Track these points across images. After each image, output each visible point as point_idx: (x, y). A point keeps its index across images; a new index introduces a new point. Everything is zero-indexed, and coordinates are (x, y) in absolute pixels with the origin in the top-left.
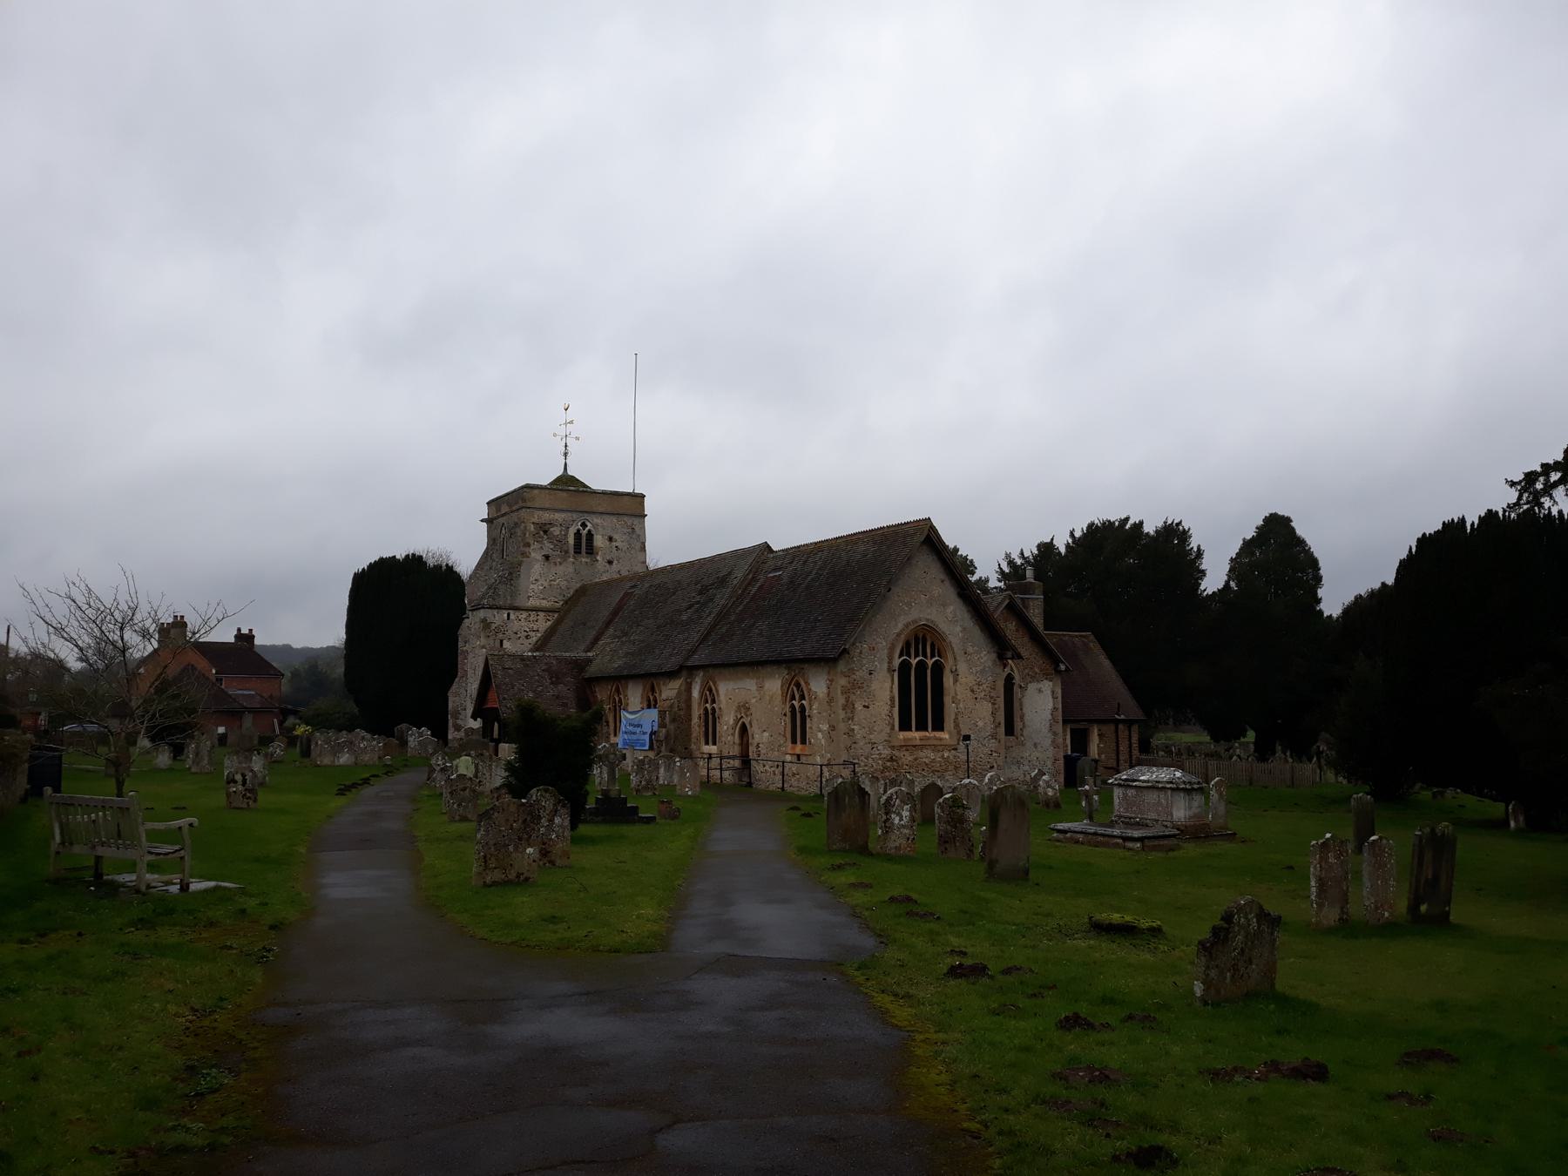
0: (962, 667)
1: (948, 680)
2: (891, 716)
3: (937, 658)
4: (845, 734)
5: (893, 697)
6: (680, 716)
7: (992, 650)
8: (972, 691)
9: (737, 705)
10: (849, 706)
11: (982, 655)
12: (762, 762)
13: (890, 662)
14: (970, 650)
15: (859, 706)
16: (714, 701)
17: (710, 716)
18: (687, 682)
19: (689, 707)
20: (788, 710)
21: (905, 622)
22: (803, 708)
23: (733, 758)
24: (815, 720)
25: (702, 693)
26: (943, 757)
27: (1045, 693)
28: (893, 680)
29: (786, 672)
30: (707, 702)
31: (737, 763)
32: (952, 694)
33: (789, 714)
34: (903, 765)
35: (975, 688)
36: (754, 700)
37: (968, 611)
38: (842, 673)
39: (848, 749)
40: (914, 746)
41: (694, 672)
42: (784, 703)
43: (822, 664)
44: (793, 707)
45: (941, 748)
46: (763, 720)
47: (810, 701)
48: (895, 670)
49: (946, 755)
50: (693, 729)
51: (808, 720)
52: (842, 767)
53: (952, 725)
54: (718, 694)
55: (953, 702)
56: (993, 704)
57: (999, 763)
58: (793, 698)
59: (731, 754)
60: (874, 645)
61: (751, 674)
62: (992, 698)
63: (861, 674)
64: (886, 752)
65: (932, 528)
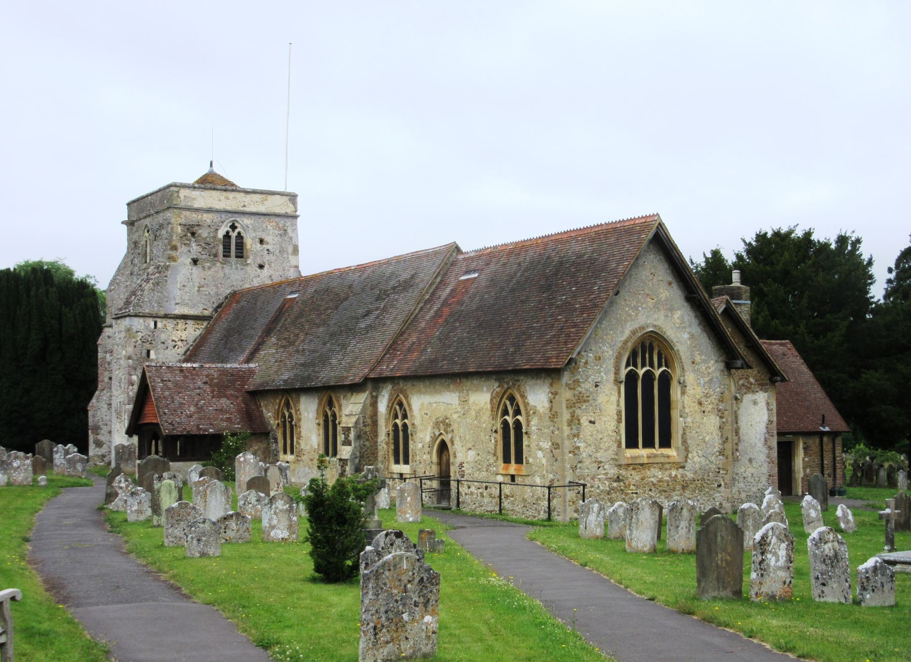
0: (690, 378)
1: (675, 393)
2: (618, 433)
3: (664, 368)
4: (570, 452)
5: (620, 412)
6: (365, 433)
7: (720, 359)
8: (700, 404)
9: (434, 420)
10: (574, 421)
11: (709, 365)
12: (466, 483)
13: (617, 372)
14: (698, 359)
15: (584, 421)
16: (405, 416)
17: (401, 434)
18: (372, 397)
19: (375, 423)
20: (499, 426)
21: (631, 329)
22: (518, 425)
23: (431, 479)
24: (534, 437)
25: (390, 408)
26: (670, 476)
27: (760, 405)
28: (619, 393)
29: (497, 384)
30: (396, 417)
31: (435, 484)
32: (680, 406)
33: (500, 431)
34: (629, 485)
35: (703, 400)
37: (696, 317)
38: (567, 385)
39: (574, 468)
40: (642, 465)
41: (381, 385)
42: (494, 418)
43: (543, 375)
44: (505, 424)
45: (667, 466)
46: (467, 438)
47: (528, 415)
48: (621, 382)
49: (674, 473)
50: (380, 448)
51: (525, 438)
52: (567, 488)
53: (680, 442)
54: (411, 409)
55: (681, 416)
56: (721, 417)
57: (726, 481)
58: (505, 412)
59: (428, 474)
60: (600, 354)
61: (451, 386)
62: (719, 411)
63: (587, 386)
64: (613, 471)
65: (661, 225)
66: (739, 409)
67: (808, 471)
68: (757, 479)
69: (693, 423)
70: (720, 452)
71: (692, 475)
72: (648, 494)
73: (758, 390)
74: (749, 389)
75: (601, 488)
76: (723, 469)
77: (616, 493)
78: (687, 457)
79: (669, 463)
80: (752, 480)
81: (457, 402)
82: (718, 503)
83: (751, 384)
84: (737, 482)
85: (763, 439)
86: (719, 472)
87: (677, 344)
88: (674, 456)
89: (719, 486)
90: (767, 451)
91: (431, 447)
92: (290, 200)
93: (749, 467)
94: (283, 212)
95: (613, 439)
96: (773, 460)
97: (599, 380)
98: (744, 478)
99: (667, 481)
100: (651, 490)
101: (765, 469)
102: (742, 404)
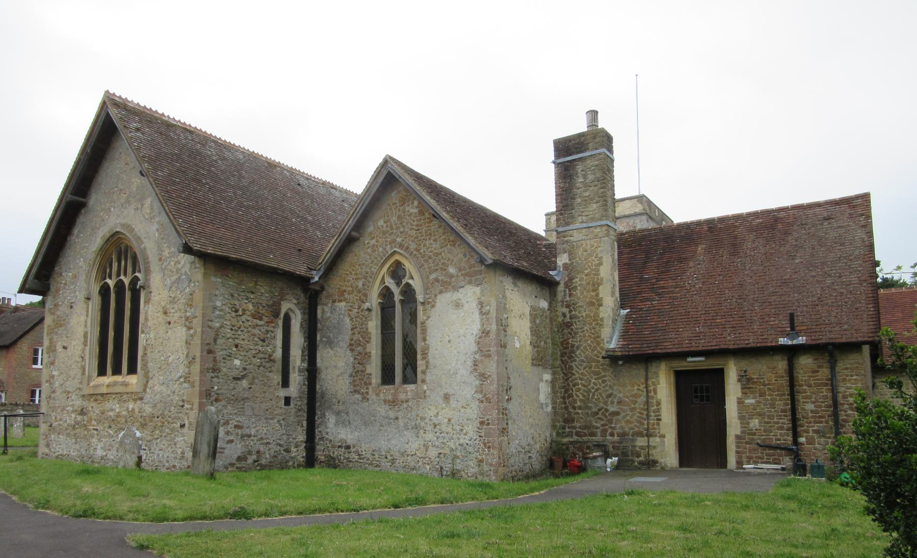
8: (165, 313)
15: (59, 349)
34: (91, 420)
40: (102, 395)
49: (131, 406)
56: (189, 328)
57: (190, 420)
63: (63, 310)
64: (78, 403)
66: (429, 317)
67: (755, 423)
68: (458, 428)
69: (155, 339)
70: (186, 378)
71: (150, 410)
72: (107, 432)
73: (463, 284)
74: (448, 285)
75: (68, 421)
76: (188, 402)
77: (80, 428)
78: (146, 386)
79: (128, 393)
80: (450, 430)
82: (179, 451)
83: (451, 276)
84: (422, 431)
85: (470, 363)
86: (183, 406)
87: (144, 240)
88: (132, 385)
89: (182, 426)
90: (477, 382)
92: (638, 201)
93: (443, 409)
94: (632, 212)
95: (79, 365)
96: (490, 396)
97: (73, 300)
98: (435, 426)
99: (125, 417)
100: (110, 427)
101: (473, 411)
102: (433, 309)
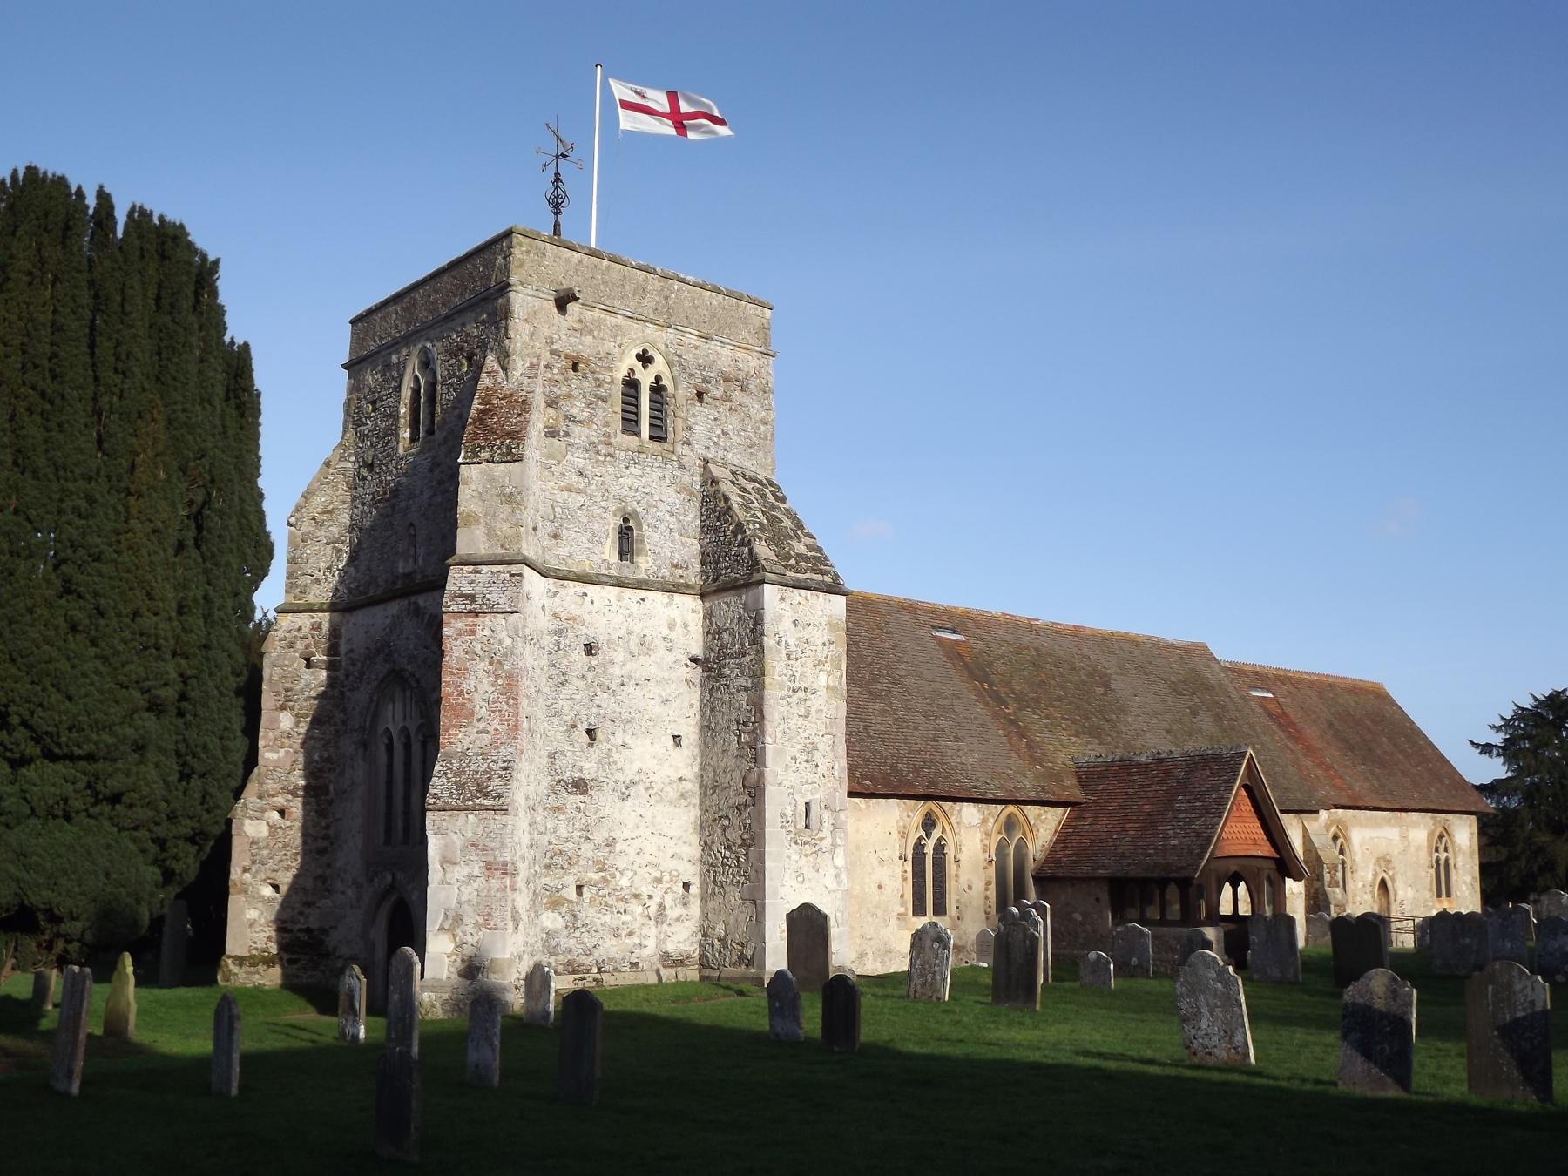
36: (1396, 852)
81: (1398, 838)
91: (1372, 885)
